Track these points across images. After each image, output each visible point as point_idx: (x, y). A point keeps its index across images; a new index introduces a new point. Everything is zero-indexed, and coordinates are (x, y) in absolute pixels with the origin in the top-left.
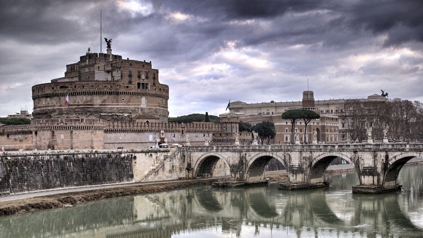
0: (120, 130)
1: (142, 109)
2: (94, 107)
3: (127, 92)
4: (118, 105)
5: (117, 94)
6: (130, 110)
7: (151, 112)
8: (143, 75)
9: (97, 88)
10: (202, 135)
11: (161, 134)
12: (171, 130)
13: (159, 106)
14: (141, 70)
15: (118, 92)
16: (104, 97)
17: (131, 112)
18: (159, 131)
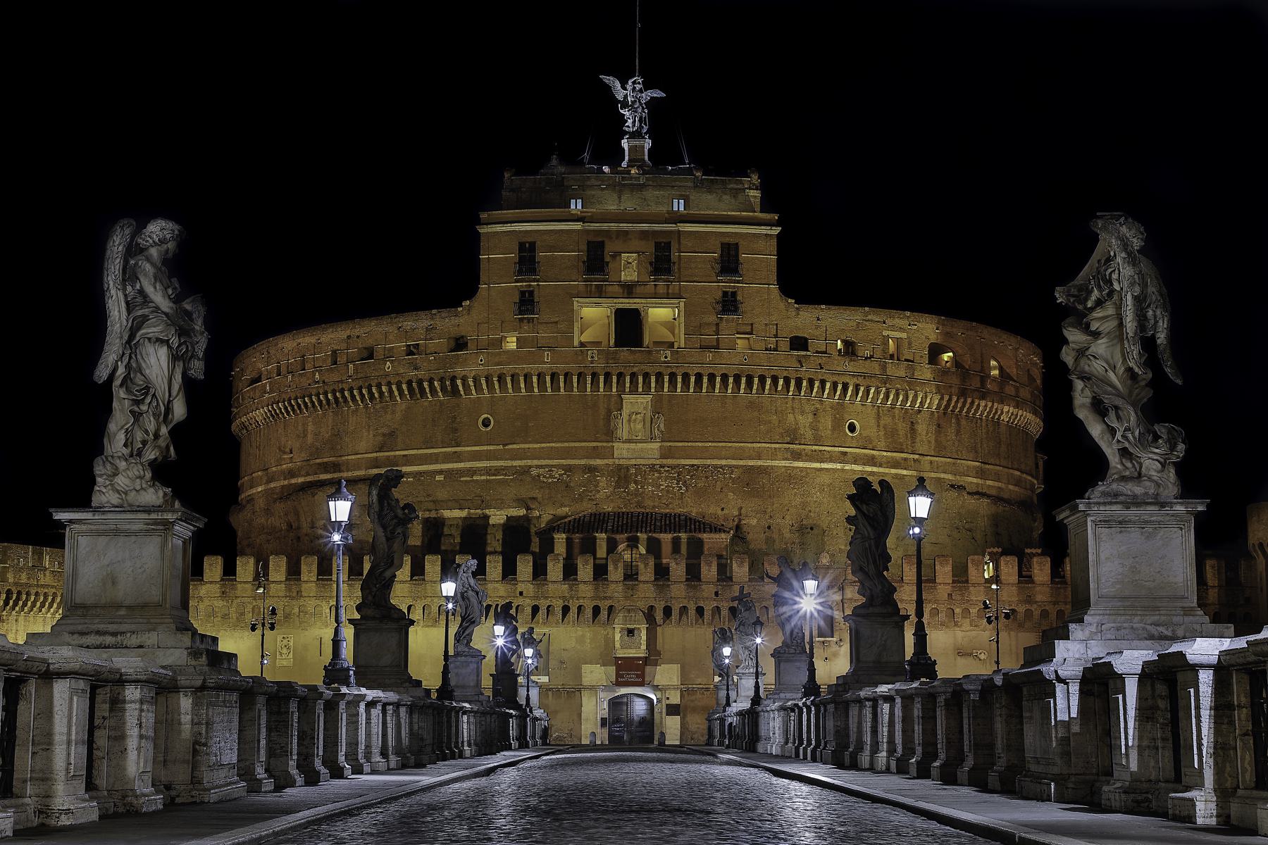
1: (622, 475)
4: (457, 457)
12: (708, 607)
13: (797, 456)
15: (453, 379)
16: (389, 416)
18: (604, 614)
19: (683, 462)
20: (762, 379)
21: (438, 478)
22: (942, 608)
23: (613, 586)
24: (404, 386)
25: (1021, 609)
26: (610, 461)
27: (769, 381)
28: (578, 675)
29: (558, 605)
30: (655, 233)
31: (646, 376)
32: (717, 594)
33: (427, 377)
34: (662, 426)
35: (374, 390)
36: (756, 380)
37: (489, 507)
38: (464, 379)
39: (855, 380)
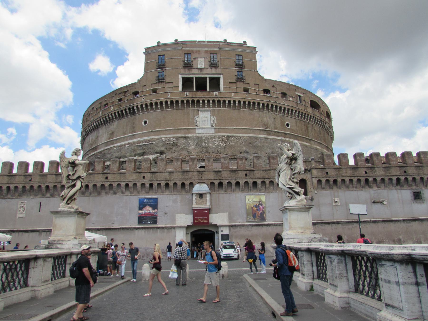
0: (20, 186)
1: (199, 140)
2: (99, 151)
3: (151, 104)
4: (134, 137)
5: (132, 111)
6: (161, 144)
7: (230, 147)
8: (199, 59)
9: (101, 112)
10: (406, 194)
11: (194, 198)
12: (242, 182)
13: (268, 133)
14: (195, 49)
15: (133, 107)
17: (162, 149)
18: (187, 187)
19: (224, 134)
20: (254, 103)
21: (127, 146)
22: (363, 179)
23: (190, 173)
24: (117, 114)
25: (402, 178)
26: (194, 135)
27: (256, 104)
28: (173, 220)
29: (163, 184)
30: (210, 51)
31: (209, 101)
32: (246, 175)
33: (124, 109)
34: (215, 121)
35: (107, 117)
36: (252, 103)
37: (145, 155)
38: (137, 107)
39: (288, 107)
